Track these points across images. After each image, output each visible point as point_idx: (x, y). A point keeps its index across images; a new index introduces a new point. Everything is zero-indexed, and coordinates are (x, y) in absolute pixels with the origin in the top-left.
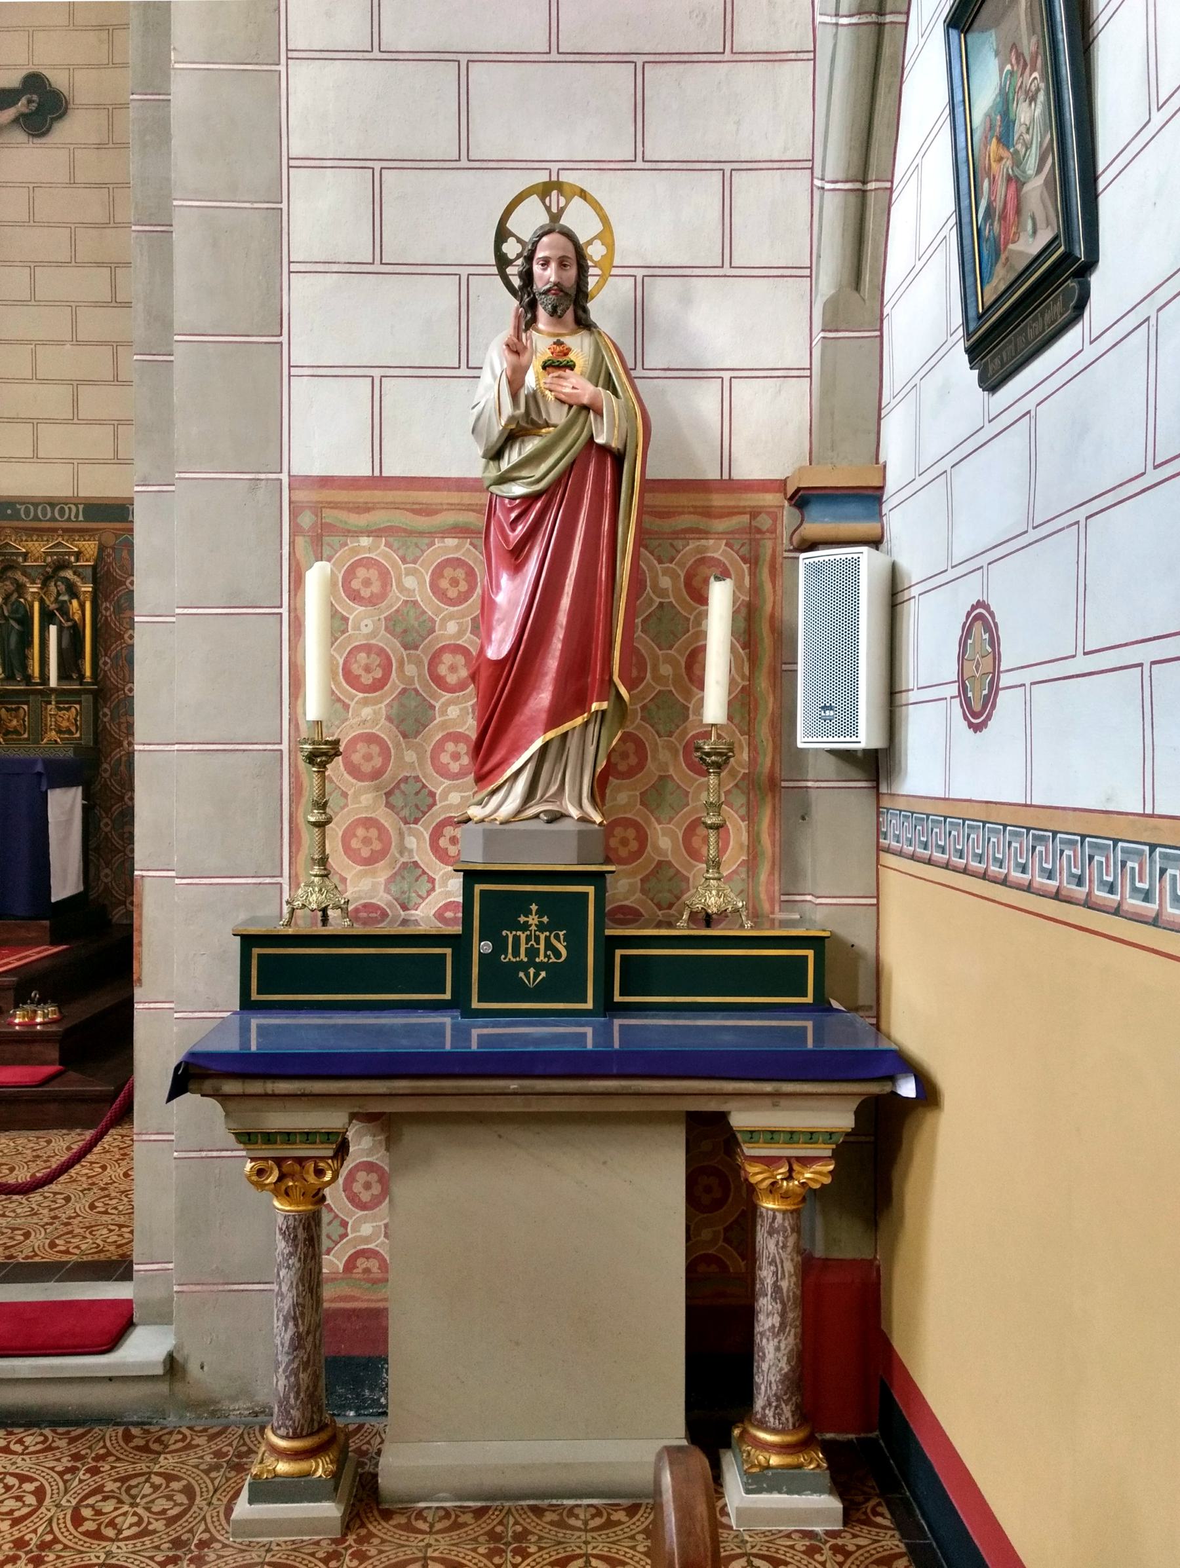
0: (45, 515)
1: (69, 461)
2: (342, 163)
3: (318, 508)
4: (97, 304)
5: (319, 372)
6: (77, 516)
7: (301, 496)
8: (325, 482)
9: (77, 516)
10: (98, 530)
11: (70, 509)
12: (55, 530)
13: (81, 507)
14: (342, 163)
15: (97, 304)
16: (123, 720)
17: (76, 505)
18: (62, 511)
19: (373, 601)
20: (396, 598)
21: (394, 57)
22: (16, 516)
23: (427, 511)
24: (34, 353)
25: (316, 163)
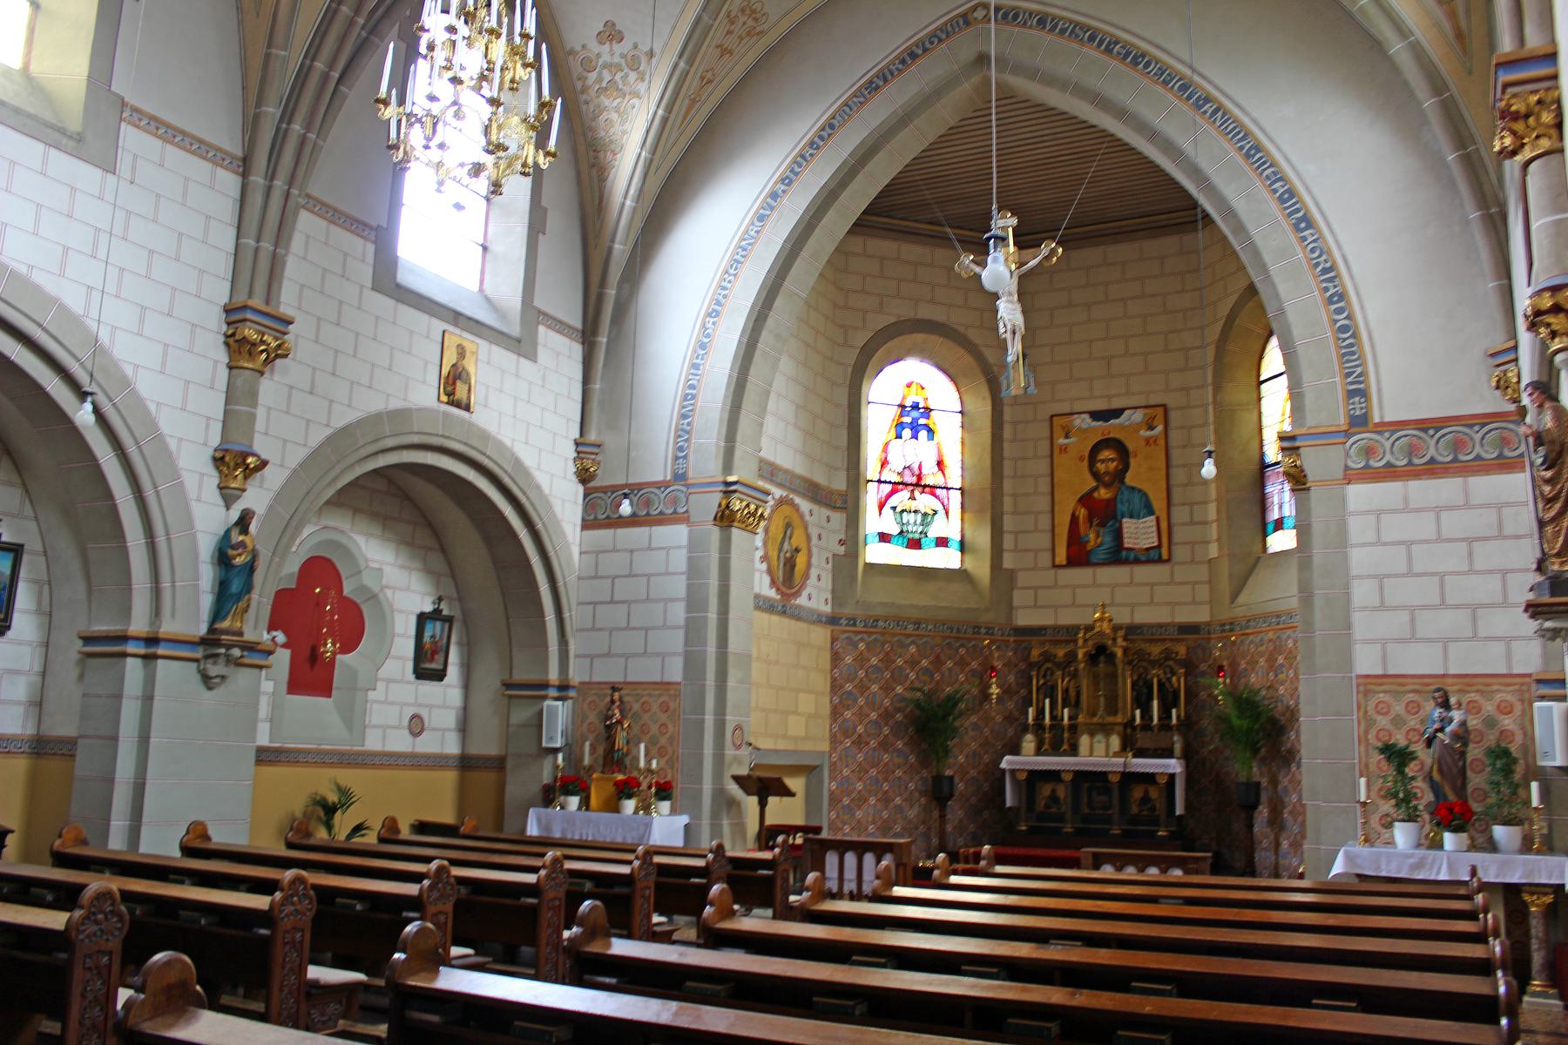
2: (1369, 577)
3: (1365, 684)
7: (1361, 681)
12: (1164, 640)
14: (1369, 577)
19: (1386, 714)
21: (1385, 544)
22: (1142, 633)
25: (1361, 577)
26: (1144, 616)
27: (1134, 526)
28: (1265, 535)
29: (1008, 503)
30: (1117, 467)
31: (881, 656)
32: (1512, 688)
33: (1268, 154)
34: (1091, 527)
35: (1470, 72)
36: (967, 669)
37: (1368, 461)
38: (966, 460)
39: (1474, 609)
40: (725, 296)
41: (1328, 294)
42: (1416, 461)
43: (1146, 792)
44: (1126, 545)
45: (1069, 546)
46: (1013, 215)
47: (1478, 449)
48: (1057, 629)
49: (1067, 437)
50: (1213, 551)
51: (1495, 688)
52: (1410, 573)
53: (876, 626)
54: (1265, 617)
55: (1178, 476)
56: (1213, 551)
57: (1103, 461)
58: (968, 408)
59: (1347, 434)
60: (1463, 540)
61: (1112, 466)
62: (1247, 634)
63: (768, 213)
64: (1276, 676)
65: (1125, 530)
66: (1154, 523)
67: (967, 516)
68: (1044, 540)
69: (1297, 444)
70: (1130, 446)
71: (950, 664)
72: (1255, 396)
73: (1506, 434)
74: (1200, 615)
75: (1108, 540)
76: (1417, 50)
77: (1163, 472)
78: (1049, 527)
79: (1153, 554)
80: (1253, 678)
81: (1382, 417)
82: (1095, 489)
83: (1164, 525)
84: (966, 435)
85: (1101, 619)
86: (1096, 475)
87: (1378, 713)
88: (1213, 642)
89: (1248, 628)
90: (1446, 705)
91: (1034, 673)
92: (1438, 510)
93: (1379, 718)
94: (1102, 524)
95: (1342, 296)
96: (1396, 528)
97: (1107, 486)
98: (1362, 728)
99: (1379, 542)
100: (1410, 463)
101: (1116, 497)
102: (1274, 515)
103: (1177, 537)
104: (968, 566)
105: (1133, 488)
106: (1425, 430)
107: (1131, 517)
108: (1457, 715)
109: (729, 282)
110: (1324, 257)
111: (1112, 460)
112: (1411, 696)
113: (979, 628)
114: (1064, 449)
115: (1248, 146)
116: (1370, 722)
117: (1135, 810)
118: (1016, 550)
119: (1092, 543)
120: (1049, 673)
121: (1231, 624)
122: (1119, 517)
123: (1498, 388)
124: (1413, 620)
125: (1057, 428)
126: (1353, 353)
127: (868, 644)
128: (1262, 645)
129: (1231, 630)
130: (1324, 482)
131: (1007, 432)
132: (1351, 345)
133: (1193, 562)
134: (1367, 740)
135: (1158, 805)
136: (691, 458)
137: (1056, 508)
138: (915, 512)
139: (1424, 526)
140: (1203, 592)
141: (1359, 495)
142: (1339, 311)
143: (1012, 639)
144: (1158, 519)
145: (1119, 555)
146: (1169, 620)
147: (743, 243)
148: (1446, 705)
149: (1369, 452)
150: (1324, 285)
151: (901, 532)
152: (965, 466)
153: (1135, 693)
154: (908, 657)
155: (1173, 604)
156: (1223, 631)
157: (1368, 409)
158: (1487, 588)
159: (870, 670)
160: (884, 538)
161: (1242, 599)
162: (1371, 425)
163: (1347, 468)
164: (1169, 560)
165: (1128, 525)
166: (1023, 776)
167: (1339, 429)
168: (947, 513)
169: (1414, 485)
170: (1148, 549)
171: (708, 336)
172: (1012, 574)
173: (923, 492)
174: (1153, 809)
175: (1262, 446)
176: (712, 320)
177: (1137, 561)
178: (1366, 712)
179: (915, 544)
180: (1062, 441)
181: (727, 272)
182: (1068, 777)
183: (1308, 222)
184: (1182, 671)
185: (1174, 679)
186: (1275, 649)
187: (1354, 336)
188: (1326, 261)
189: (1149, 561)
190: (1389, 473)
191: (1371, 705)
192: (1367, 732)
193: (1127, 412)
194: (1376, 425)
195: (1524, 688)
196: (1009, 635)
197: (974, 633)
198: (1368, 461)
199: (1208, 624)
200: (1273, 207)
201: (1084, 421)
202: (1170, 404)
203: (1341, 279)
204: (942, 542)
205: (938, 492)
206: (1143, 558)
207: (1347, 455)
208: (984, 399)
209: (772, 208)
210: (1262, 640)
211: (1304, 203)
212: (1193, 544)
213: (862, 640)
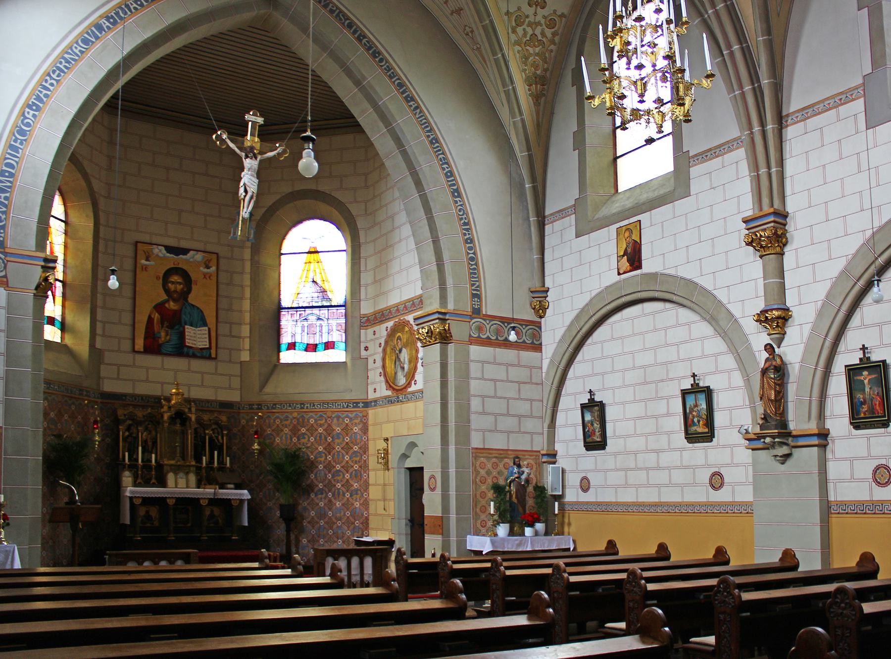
1: (214, 387)
3: (476, 453)
5: (477, 430)
7: (473, 451)
8: (477, 448)
18: (211, 405)
19: (483, 469)
20: (487, 468)
23: (490, 454)
25: (475, 396)
26: (197, 393)
27: (192, 332)
28: (279, 351)
30: (182, 289)
32: (532, 457)
33: (442, 146)
34: (162, 327)
35: (539, 145)
37: (479, 334)
38: (69, 260)
39: (520, 417)
40: (46, 96)
41: (466, 237)
42: (499, 338)
44: (187, 344)
45: (146, 338)
46: (261, 116)
47: (524, 337)
49: (147, 260)
50: (245, 356)
51: (527, 457)
52: (495, 397)
54: (290, 404)
55: (224, 303)
56: (245, 356)
57: (173, 283)
58: (73, 219)
59: (472, 318)
60: (517, 382)
61: (180, 287)
62: (274, 412)
63: (94, 40)
65: (186, 334)
66: (207, 332)
68: (126, 332)
69: (447, 317)
70: (193, 276)
72: (278, 263)
73: (535, 332)
74: (234, 396)
75: (175, 339)
76: (523, 121)
77: (215, 299)
78: (131, 322)
79: (205, 353)
80: (278, 440)
81: (486, 312)
82: (167, 301)
83: (213, 334)
84: (69, 241)
85: (177, 394)
86: (167, 291)
87: (481, 468)
88: (242, 415)
89: (275, 408)
90: (519, 466)
92: (508, 365)
93: (481, 471)
94: (171, 327)
95: (472, 241)
96: (492, 371)
97: (175, 300)
98: (474, 475)
99: (482, 378)
100: (497, 339)
101: (181, 310)
102: (286, 339)
103: (220, 344)
105: (193, 306)
106: (503, 323)
107: (192, 326)
108: (526, 470)
109: (52, 85)
110: (465, 216)
111: (180, 283)
112: (494, 460)
114: (145, 268)
115: (432, 137)
116: (478, 473)
118: (103, 335)
119: (163, 339)
121: (259, 405)
122: (183, 324)
123: (534, 309)
124: (496, 421)
125: (140, 252)
126: (475, 274)
129: (258, 409)
130: (460, 342)
131: (101, 248)
132: (474, 269)
133: (230, 361)
134: (476, 482)
136: (10, 230)
137: (136, 309)
139: (499, 373)
140: (236, 382)
141: (475, 351)
142: (470, 248)
144: (209, 329)
145: (181, 350)
146: (213, 398)
147: (66, 56)
148: (519, 466)
149: (480, 329)
150: (464, 232)
152: (68, 265)
157: (481, 305)
158: (523, 408)
161: (269, 389)
162: (481, 315)
163: (470, 336)
164: (215, 358)
165: (189, 330)
167: (465, 313)
169: (498, 350)
170: (202, 349)
171: (28, 125)
175: (280, 294)
176: (32, 112)
177: (194, 356)
178: (476, 467)
180: (144, 262)
181: (49, 75)
183: (460, 196)
186: (298, 424)
187: (476, 264)
188: (465, 218)
189: (203, 357)
190: (487, 342)
191: (478, 463)
192: (476, 478)
193: (192, 253)
194: (484, 315)
195: (537, 457)
198: (479, 334)
199: (238, 403)
200: (443, 178)
201: (160, 251)
202: (221, 254)
203: (472, 231)
206: (199, 355)
207: (471, 328)
208: (87, 216)
209: (97, 38)
210: (287, 417)
211: (457, 182)
212: (231, 350)
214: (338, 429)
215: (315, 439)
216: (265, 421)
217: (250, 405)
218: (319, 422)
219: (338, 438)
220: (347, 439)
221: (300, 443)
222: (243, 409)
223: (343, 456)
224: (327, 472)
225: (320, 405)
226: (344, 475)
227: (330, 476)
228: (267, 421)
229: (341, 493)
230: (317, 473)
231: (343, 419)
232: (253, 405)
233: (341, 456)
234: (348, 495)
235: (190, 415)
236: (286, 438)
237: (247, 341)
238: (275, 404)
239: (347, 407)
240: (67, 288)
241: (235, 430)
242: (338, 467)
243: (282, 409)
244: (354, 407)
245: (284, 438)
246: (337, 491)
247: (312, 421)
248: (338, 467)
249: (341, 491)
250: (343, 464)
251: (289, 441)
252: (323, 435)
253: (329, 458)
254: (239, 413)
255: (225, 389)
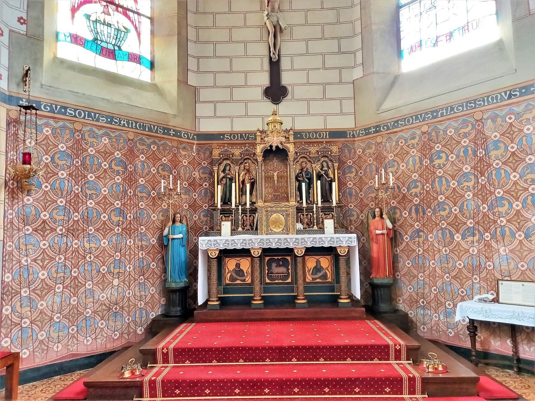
0: (313, 136)
4: (333, 53)
6: (326, 136)
9: (326, 136)
10: (335, 141)
11: (323, 134)
13: (328, 133)
15: (333, 53)
16: (348, 218)
17: (326, 132)
18: (320, 135)
22: (301, 137)
24: (308, 74)
26: (303, 124)
29: (191, 34)
31: (70, 144)
36: (158, 164)
43: (318, 262)
48: (233, 135)
53: (65, 114)
64: (432, 161)
67: (156, 40)
71: (142, 157)
89: (397, 127)
91: (215, 168)
104: (158, 80)
113: (170, 130)
117: (309, 278)
120: (228, 168)
127: (53, 129)
128: (414, 138)
129: (376, 132)
135: (329, 275)
138: (109, 25)
140: (348, 107)
143: (196, 142)
151: (96, 39)
153: (297, 183)
154: (100, 147)
155: (325, 115)
156: (369, 133)
159: (57, 156)
160: (76, 39)
166: (214, 254)
168: (139, 34)
172: (195, 90)
173: (117, 10)
174: (325, 276)
179: (111, 54)
182: (256, 253)
184: (336, 165)
185: (330, 172)
196: (193, 139)
197: (164, 134)
204: (135, 58)
205: (131, 14)
210: (414, 134)
213: (47, 125)
214: (494, 135)
215: (458, 156)
216: (385, 146)
217: (365, 129)
218: (462, 131)
219: (497, 148)
220: (513, 147)
221: (434, 166)
222: (358, 136)
223: (508, 175)
224: (480, 202)
225: (462, 106)
226: (511, 204)
227: (484, 208)
228: (388, 145)
229: (508, 233)
230: (463, 203)
231: (503, 118)
232: (370, 128)
233: (503, 175)
234: (520, 236)
235: (288, 145)
236: (414, 161)
237: (359, 54)
238: (397, 122)
239: (510, 97)
240: (155, 24)
241: (350, 163)
242: (499, 193)
243: (406, 125)
244: (522, 94)
245: (411, 162)
246: (499, 230)
247: (451, 132)
248: (499, 193)
249: (507, 229)
250: (508, 187)
251: (419, 165)
252: (469, 149)
253: (482, 180)
254: (354, 141)
255: (337, 114)
